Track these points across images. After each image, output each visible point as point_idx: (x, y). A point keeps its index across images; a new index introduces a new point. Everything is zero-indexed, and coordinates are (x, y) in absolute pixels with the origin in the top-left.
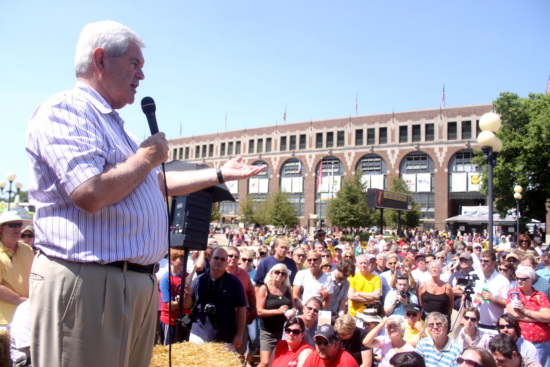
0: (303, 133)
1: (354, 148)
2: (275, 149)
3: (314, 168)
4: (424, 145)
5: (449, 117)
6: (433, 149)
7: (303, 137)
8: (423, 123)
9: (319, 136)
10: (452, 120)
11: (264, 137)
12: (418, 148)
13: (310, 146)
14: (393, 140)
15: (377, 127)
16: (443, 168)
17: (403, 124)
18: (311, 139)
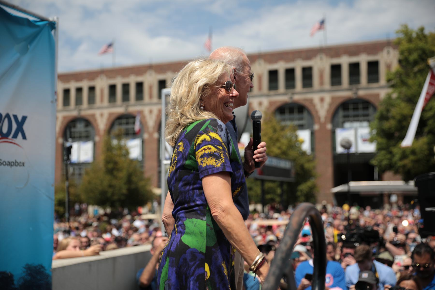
2: (102, 100)
5: (332, 56)
6: (311, 101)
7: (140, 85)
10: (336, 61)
11: (85, 85)
12: (291, 98)
13: (151, 97)
14: (260, 88)
17: (274, 67)
18: (151, 88)
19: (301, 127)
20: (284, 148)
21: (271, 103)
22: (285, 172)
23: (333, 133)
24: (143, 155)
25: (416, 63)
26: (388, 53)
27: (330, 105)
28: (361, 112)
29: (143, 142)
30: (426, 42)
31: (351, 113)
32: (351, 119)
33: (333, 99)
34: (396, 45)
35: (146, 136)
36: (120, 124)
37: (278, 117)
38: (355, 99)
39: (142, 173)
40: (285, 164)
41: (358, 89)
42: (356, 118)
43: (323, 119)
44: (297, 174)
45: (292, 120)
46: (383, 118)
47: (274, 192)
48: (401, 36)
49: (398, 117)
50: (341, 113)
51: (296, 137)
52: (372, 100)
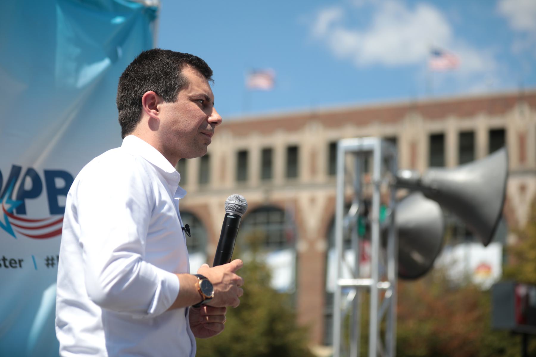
29: (298, 259)
35: (302, 246)
36: (255, 224)
39: (294, 316)
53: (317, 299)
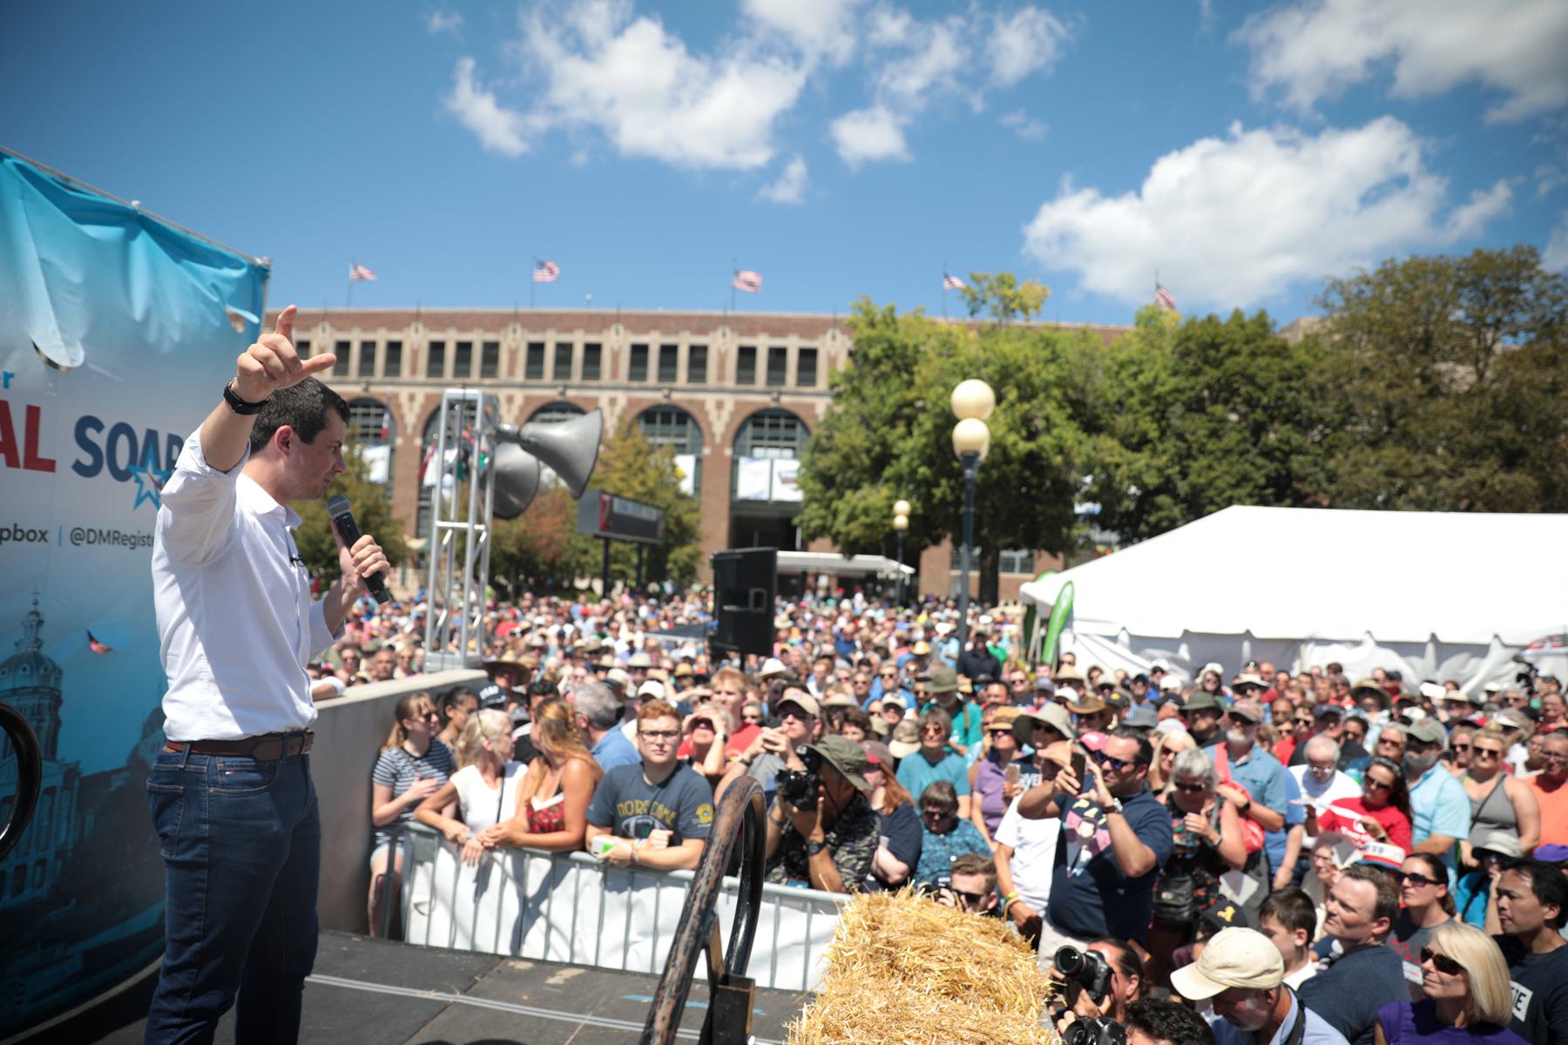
0: (396, 337)
1: (523, 386)
3: (421, 427)
4: (682, 393)
5: (742, 334)
6: (702, 404)
7: (395, 348)
8: (684, 342)
9: (437, 348)
10: (748, 342)
12: (668, 397)
13: (414, 371)
14: (614, 374)
15: (579, 340)
16: (721, 447)
17: (641, 339)
18: (415, 353)
19: (681, 449)
20: (651, 484)
21: (631, 403)
22: (647, 528)
23: (734, 463)
24: (391, 476)
25: (877, 362)
26: (834, 338)
27: (733, 415)
28: (782, 432)
29: (393, 451)
30: (896, 331)
31: (766, 431)
32: (765, 442)
33: (737, 404)
34: (850, 328)
37: (641, 427)
38: (774, 409)
39: (389, 508)
40: (648, 514)
41: (780, 393)
42: (774, 441)
43: (718, 439)
44: (668, 531)
45: (662, 435)
46: (819, 449)
47: (627, 561)
48: (860, 315)
49: (845, 449)
50: (750, 430)
51: (674, 467)
52: (802, 414)
53: (414, 493)
